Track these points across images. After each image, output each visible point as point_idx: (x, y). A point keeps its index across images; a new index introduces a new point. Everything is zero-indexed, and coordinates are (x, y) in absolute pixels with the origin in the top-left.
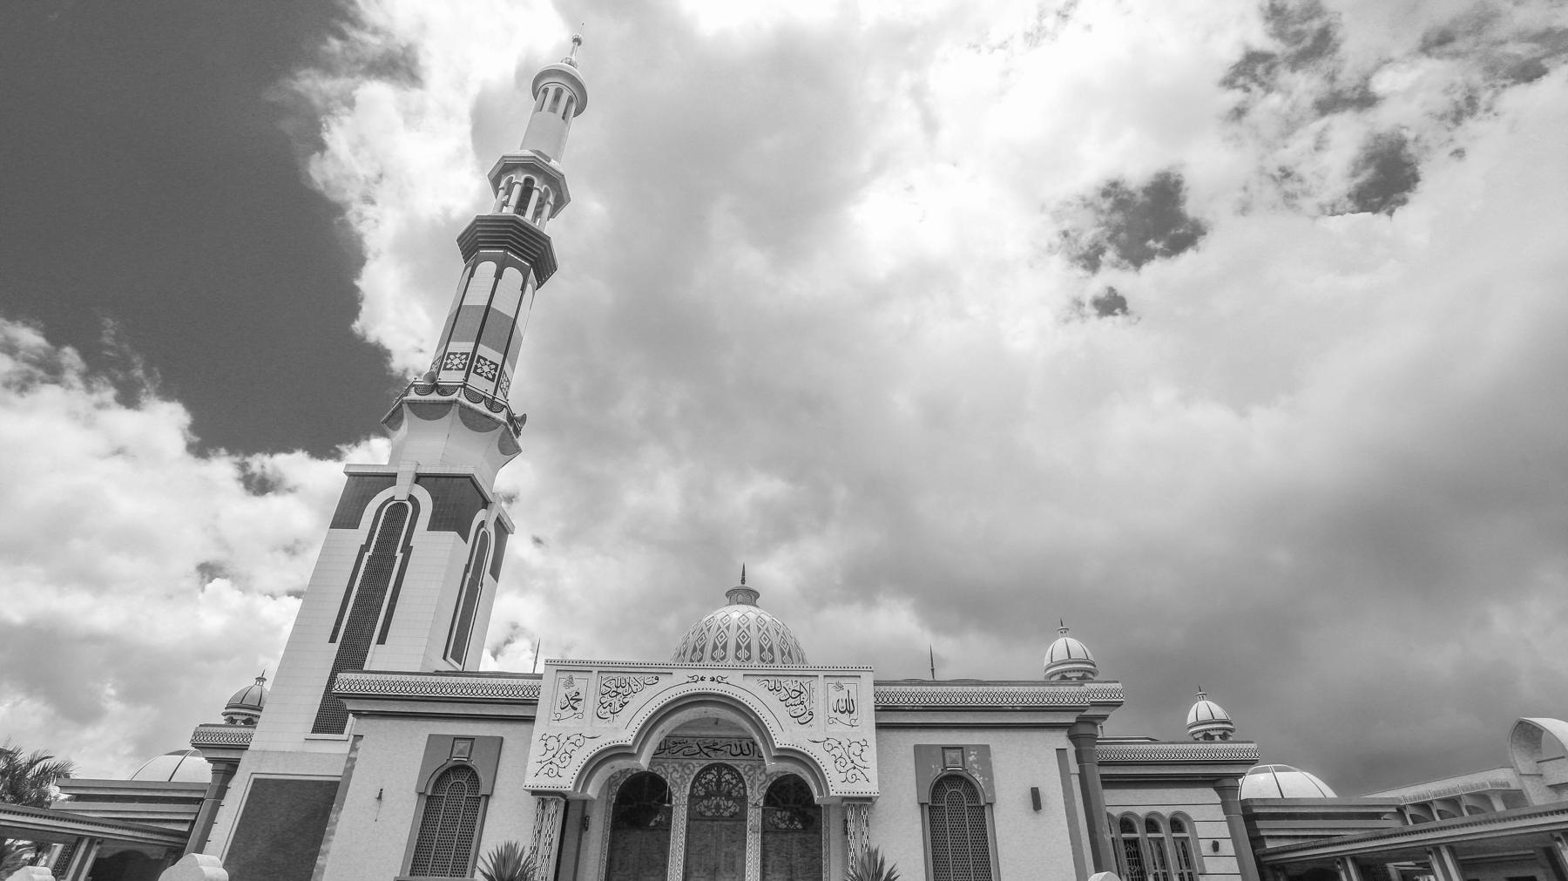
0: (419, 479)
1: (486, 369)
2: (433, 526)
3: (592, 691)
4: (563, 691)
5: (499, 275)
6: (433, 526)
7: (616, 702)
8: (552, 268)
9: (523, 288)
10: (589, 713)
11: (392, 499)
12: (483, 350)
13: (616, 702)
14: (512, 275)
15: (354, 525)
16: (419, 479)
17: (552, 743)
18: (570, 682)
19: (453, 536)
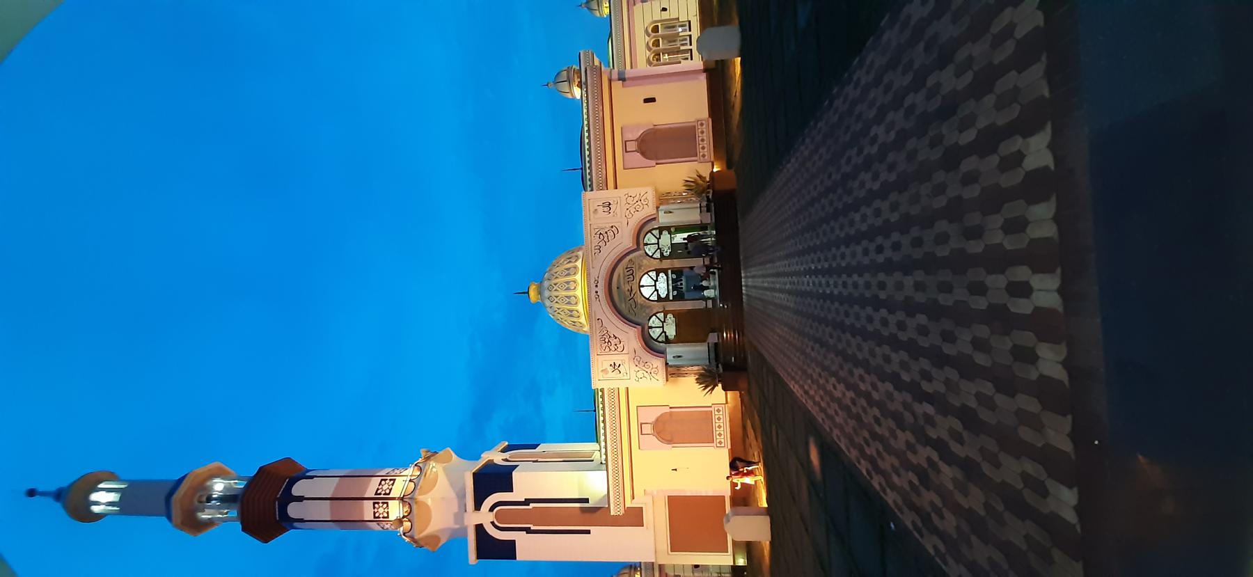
0: (478, 506)
1: (385, 487)
2: (509, 488)
3: (607, 357)
4: (611, 374)
5: (301, 499)
6: (509, 488)
7: (613, 341)
8: (288, 461)
9: (312, 477)
10: (621, 357)
11: (493, 523)
12: (370, 493)
13: (613, 341)
14: (297, 490)
15: (512, 543)
16: (478, 506)
17: (640, 374)
18: (604, 371)
19: (516, 475)
